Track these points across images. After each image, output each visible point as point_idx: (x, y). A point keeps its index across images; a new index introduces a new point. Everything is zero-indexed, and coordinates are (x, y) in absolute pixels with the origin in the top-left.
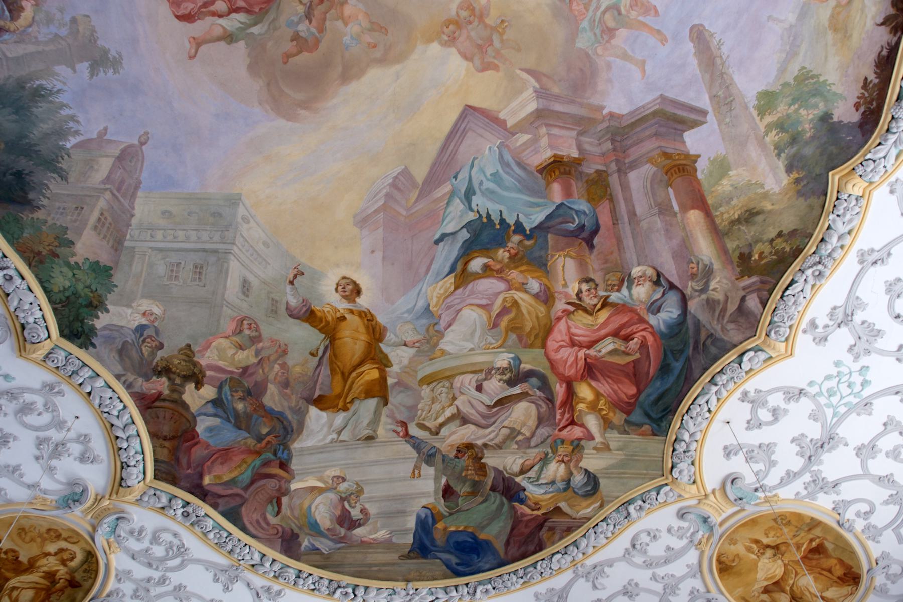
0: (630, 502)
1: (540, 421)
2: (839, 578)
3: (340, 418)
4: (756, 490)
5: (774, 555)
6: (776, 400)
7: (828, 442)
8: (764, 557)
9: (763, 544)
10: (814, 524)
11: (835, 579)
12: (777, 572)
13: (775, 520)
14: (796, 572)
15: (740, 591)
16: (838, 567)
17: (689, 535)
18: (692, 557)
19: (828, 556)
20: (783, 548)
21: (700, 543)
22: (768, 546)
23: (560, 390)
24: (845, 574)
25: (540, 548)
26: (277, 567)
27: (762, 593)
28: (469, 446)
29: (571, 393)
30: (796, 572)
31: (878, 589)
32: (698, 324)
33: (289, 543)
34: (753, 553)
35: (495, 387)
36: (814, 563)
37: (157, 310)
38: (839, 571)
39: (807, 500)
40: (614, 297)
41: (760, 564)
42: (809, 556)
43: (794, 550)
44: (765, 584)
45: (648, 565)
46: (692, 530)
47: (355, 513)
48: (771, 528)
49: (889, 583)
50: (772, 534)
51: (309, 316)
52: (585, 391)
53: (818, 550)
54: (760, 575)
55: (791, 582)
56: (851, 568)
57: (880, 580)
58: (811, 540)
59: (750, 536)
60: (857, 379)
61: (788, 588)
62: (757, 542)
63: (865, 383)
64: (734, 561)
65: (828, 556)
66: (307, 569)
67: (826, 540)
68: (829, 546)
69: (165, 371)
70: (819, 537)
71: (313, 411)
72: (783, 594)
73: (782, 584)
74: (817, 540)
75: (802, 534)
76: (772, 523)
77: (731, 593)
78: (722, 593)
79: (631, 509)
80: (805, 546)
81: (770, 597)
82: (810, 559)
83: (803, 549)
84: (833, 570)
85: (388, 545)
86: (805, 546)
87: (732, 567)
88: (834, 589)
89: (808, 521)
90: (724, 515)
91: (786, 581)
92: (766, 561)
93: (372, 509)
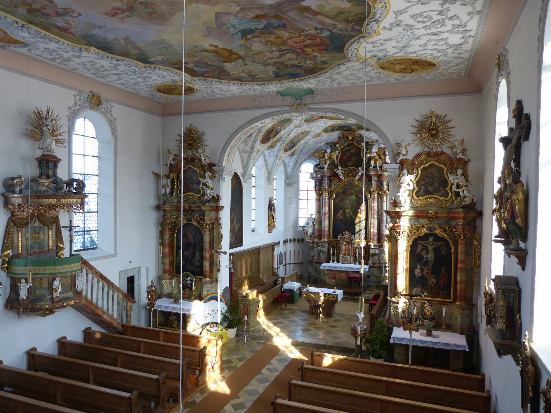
0: (340, 65)
1: (297, 56)
3: (233, 63)
6: (382, 41)
7: (407, 46)
23: (300, 51)
25: (317, 72)
26: (239, 85)
28: (278, 62)
29: (303, 51)
32: (340, 35)
33: (239, 79)
35: (276, 54)
37: (164, 57)
40: (303, 34)
45: (356, 70)
47: (253, 74)
51: (207, 51)
52: (308, 50)
60: (412, 35)
63: (414, 35)
66: (248, 83)
69: (176, 64)
71: (224, 64)
79: (341, 66)
85: (267, 77)
93: (258, 73)
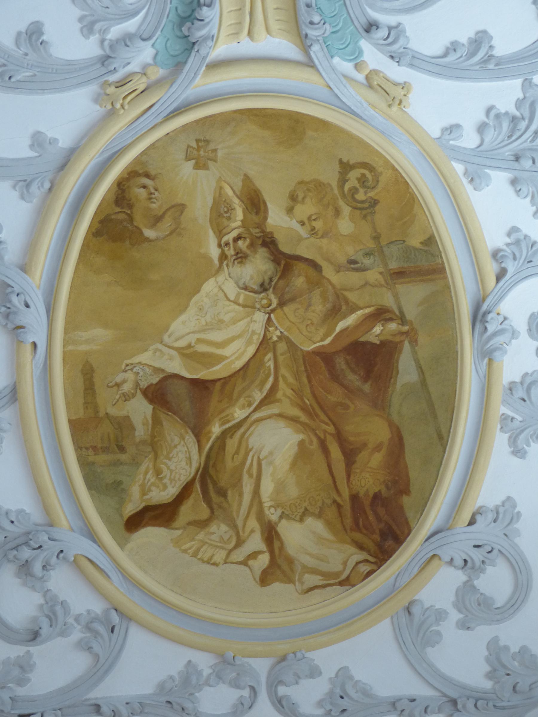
2: (354, 498)
4: (371, 27)
5: (263, 288)
8: (237, 270)
9: (261, 226)
10: (424, 265)
11: (346, 493)
12: (227, 351)
13: (345, 167)
14: (274, 389)
15: (96, 337)
16: (377, 459)
17: (115, 31)
18: (66, 113)
19: (379, 403)
20: (299, 282)
21: (120, 84)
22: (268, 242)
24: (377, 496)
27: (145, 393)
30: (274, 389)
31: (415, 610)
34: (220, 233)
36: (335, 395)
38: (369, 478)
39: (459, 168)
41: (209, 286)
42: (341, 362)
43: (319, 307)
44: (176, 366)
46: (131, 25)
48: (319, 186)
49: (455, 616)
50: (305, 209)
53: (371, 360)
54: (184, 327)
55: (239, 414)
56: (406, 491)
57: (440, 588)
58: (380, 314)
59: (251, 174)
61: (216, 429)
62: (255, 203)
64: (157, 220)
65: (379, 403)
67: (414, 342)
68: (406, 370)
70: (403, 320)
72: (190, 438)
73: (215, 397)
74: (393, 326)
75: (373, 276)
76: (330, 175)
77: (70, 326)
78: (50, 310)
80: (350, 320)
81: (156, 421)
82: (335, 376)
83: (341, 325)
84: (362, 456)
86: (350, 320)
87: (136, 238)
88: (317, 525)
89: (415, 242)
90: (245, 47)
91: (231, 400)
92: (231, 290)
